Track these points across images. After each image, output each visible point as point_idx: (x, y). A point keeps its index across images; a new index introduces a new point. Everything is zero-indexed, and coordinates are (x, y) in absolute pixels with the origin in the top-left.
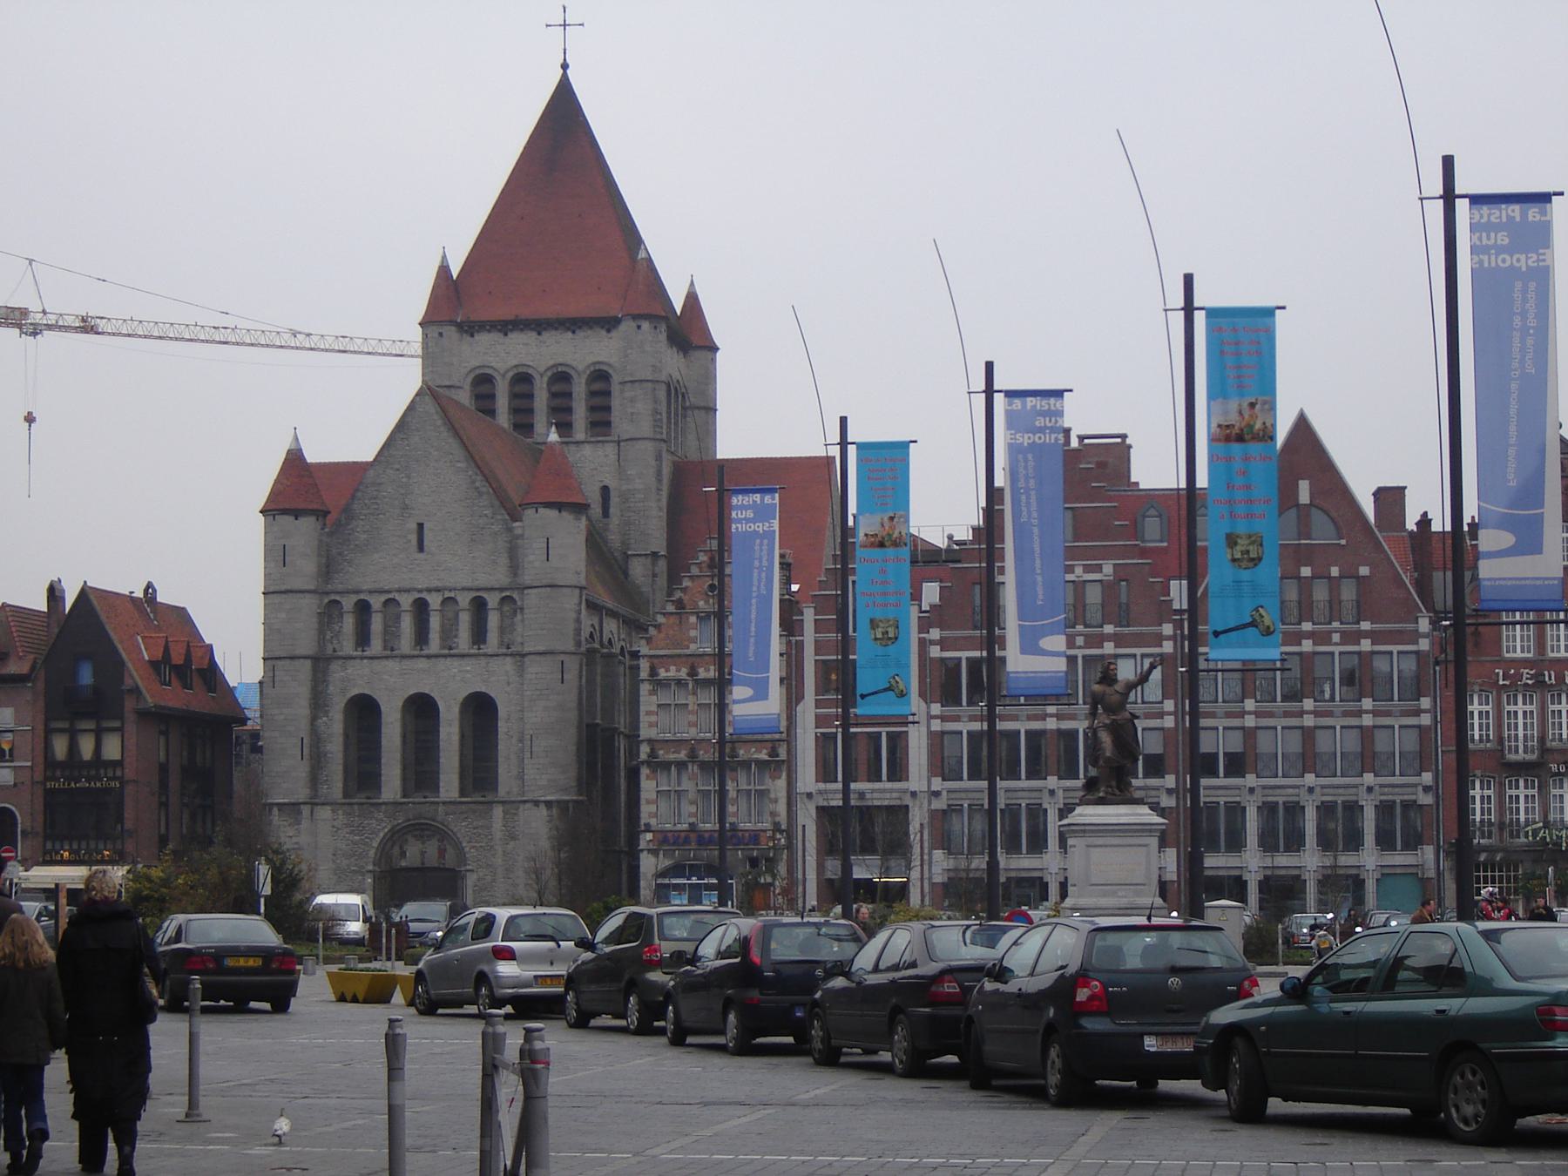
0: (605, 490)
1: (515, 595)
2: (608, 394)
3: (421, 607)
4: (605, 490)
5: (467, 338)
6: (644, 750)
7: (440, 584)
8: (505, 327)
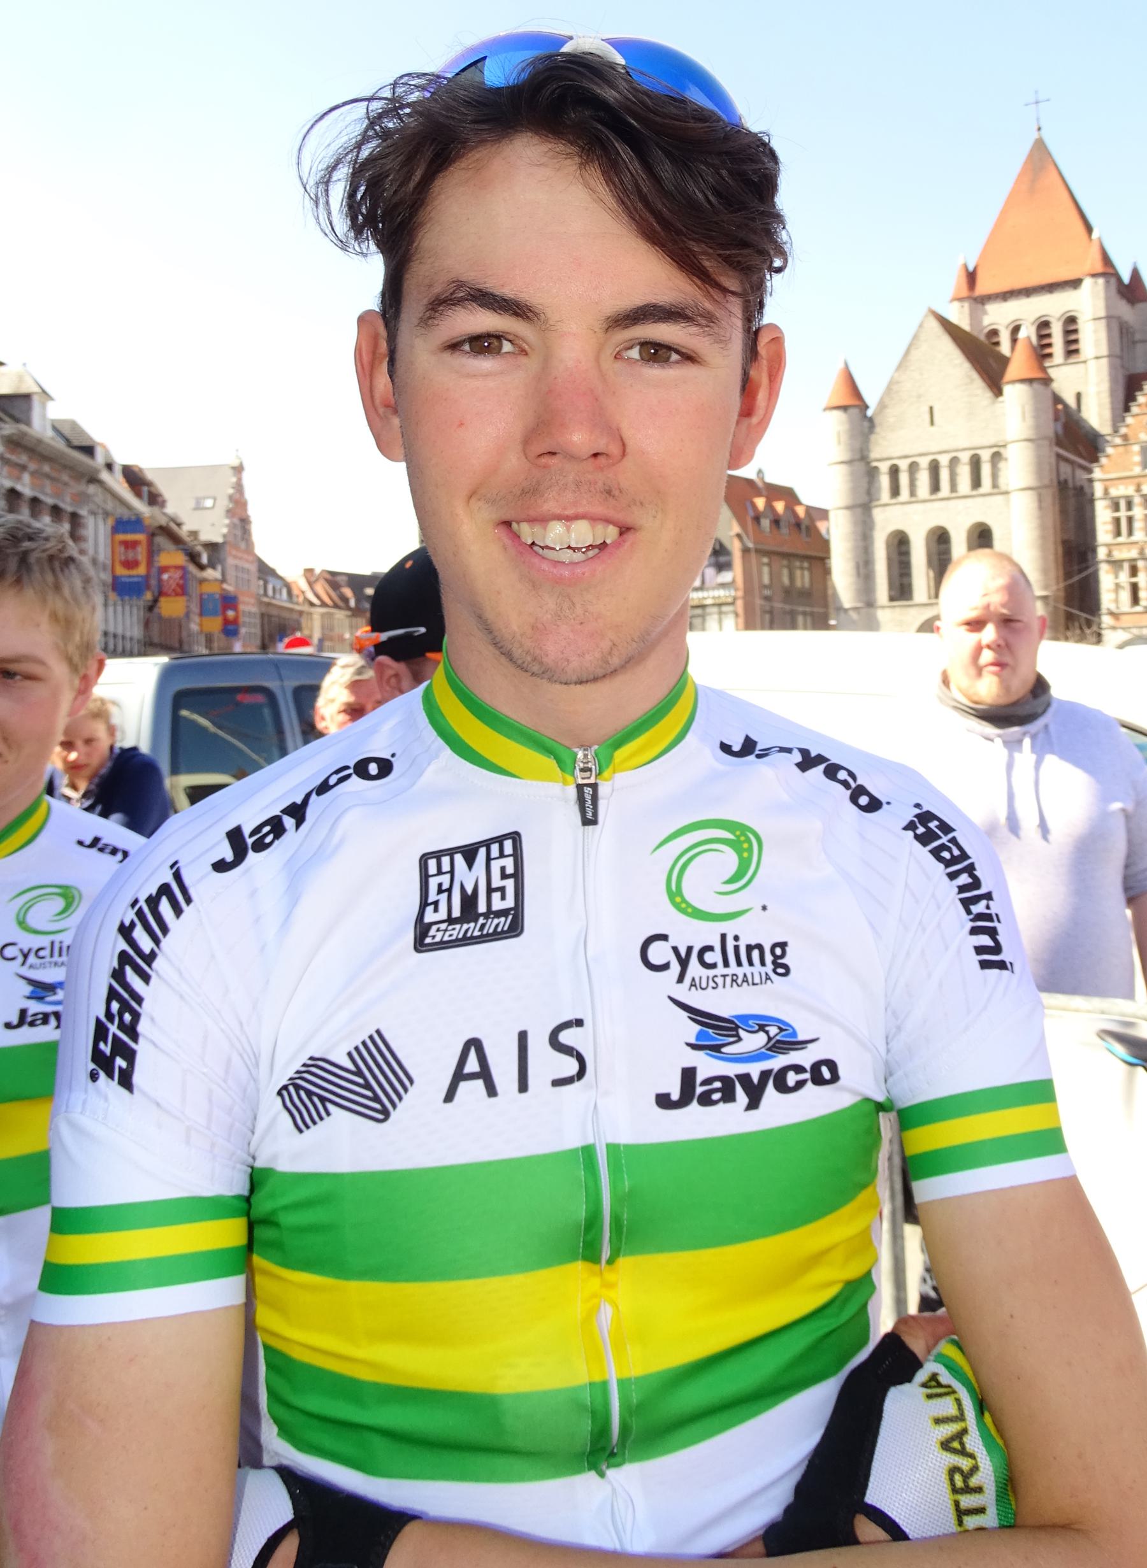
0: (1079, 396)
1: (1002, 450)
2: (1075, 331)
3: (934, 468)
4: (1079, 396)
5: (980, 306)
6: (1102, 553)
7: (945, 447)
8: (1006, 295)
